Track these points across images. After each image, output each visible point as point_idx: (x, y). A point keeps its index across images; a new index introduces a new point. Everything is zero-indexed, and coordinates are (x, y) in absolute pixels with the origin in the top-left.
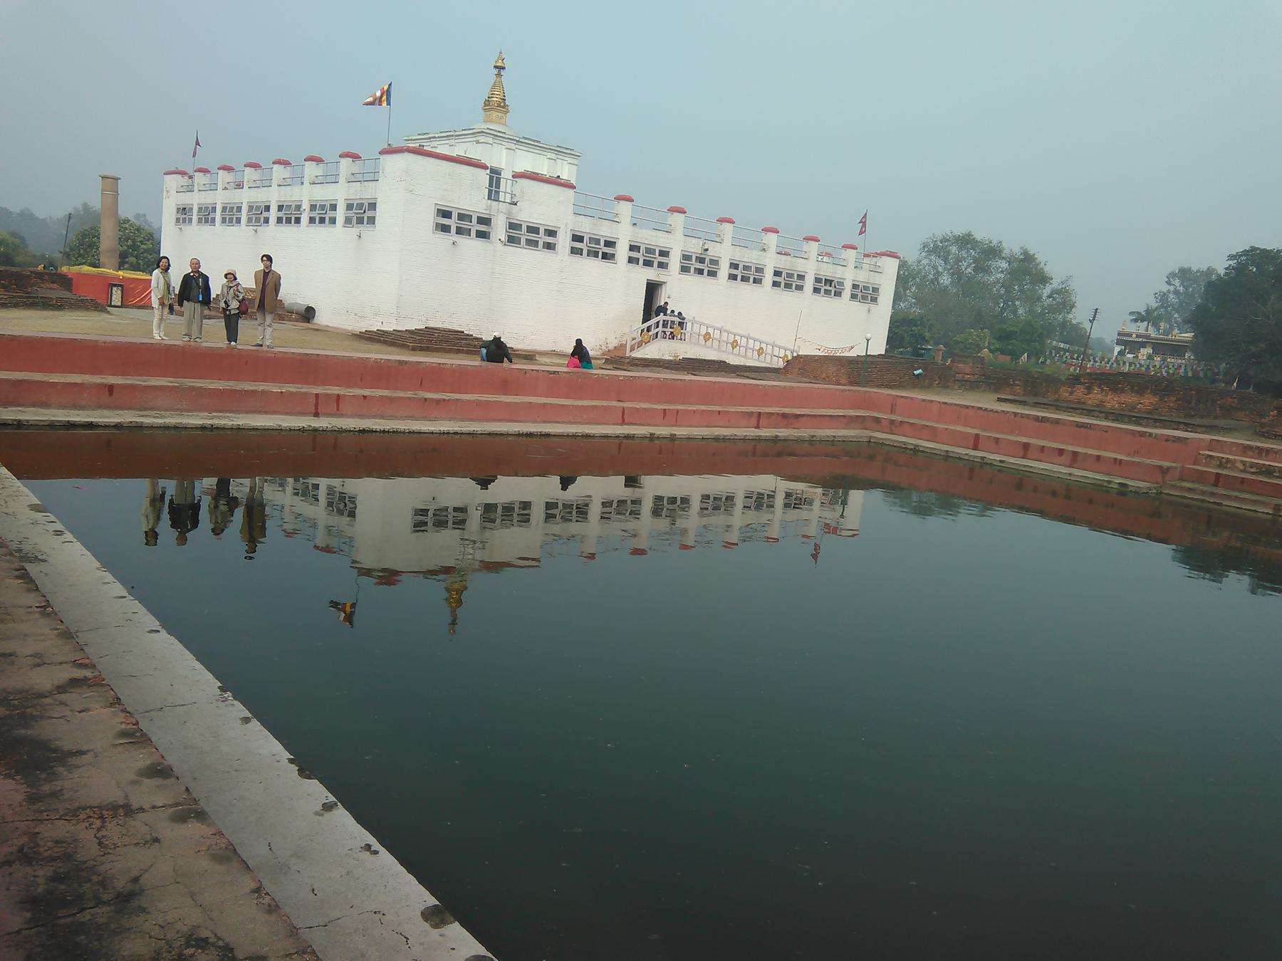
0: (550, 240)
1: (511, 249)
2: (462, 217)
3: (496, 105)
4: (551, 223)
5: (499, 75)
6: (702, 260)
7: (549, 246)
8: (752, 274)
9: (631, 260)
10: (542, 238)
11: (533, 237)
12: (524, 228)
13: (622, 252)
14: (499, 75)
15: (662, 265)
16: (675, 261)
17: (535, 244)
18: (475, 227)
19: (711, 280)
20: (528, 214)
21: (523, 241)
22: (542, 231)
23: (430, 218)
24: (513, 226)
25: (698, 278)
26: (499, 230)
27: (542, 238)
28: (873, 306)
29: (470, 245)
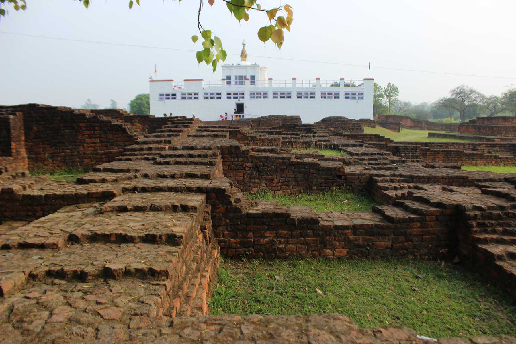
0: (196, 96)
1: (184, 101)
2: (167, 95)
3: (243, 56)
4: (196, 92)
5: (244, 47)
6: (260, 94)
7: (198, 98)
8: (286, 95)
9: (228, 98)
10: (193, 96)
11: (190, 96)
12: (187, 94)
13: (224, 96)
14: (244, 47)
15: (243, 98)
16: (247, 96)
17: (191, 98)
18: (170, 97)
19: (265, 100)
20: (187, 91)
21: (187, 98)
22: (193, 94)
23: (158, 97)
24: (183, 94)
25: (259, 99)
26: (179, 96)
27: (193, 96)
28: (360, 101)
29: (171, 101)
